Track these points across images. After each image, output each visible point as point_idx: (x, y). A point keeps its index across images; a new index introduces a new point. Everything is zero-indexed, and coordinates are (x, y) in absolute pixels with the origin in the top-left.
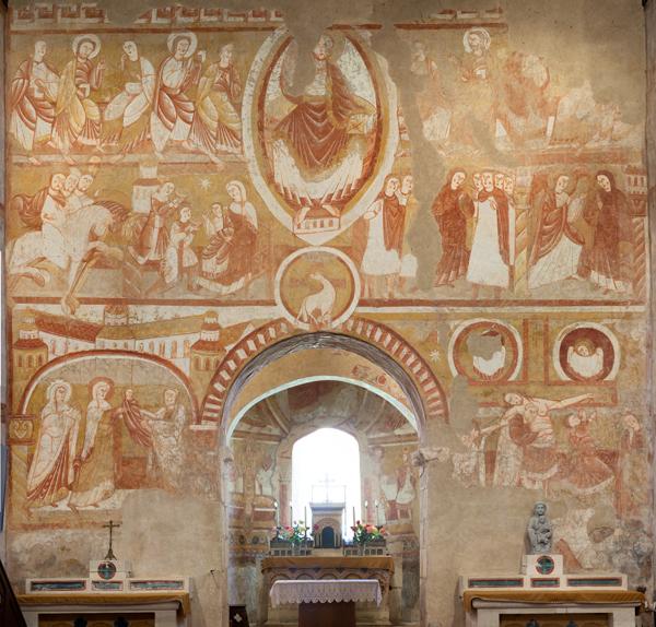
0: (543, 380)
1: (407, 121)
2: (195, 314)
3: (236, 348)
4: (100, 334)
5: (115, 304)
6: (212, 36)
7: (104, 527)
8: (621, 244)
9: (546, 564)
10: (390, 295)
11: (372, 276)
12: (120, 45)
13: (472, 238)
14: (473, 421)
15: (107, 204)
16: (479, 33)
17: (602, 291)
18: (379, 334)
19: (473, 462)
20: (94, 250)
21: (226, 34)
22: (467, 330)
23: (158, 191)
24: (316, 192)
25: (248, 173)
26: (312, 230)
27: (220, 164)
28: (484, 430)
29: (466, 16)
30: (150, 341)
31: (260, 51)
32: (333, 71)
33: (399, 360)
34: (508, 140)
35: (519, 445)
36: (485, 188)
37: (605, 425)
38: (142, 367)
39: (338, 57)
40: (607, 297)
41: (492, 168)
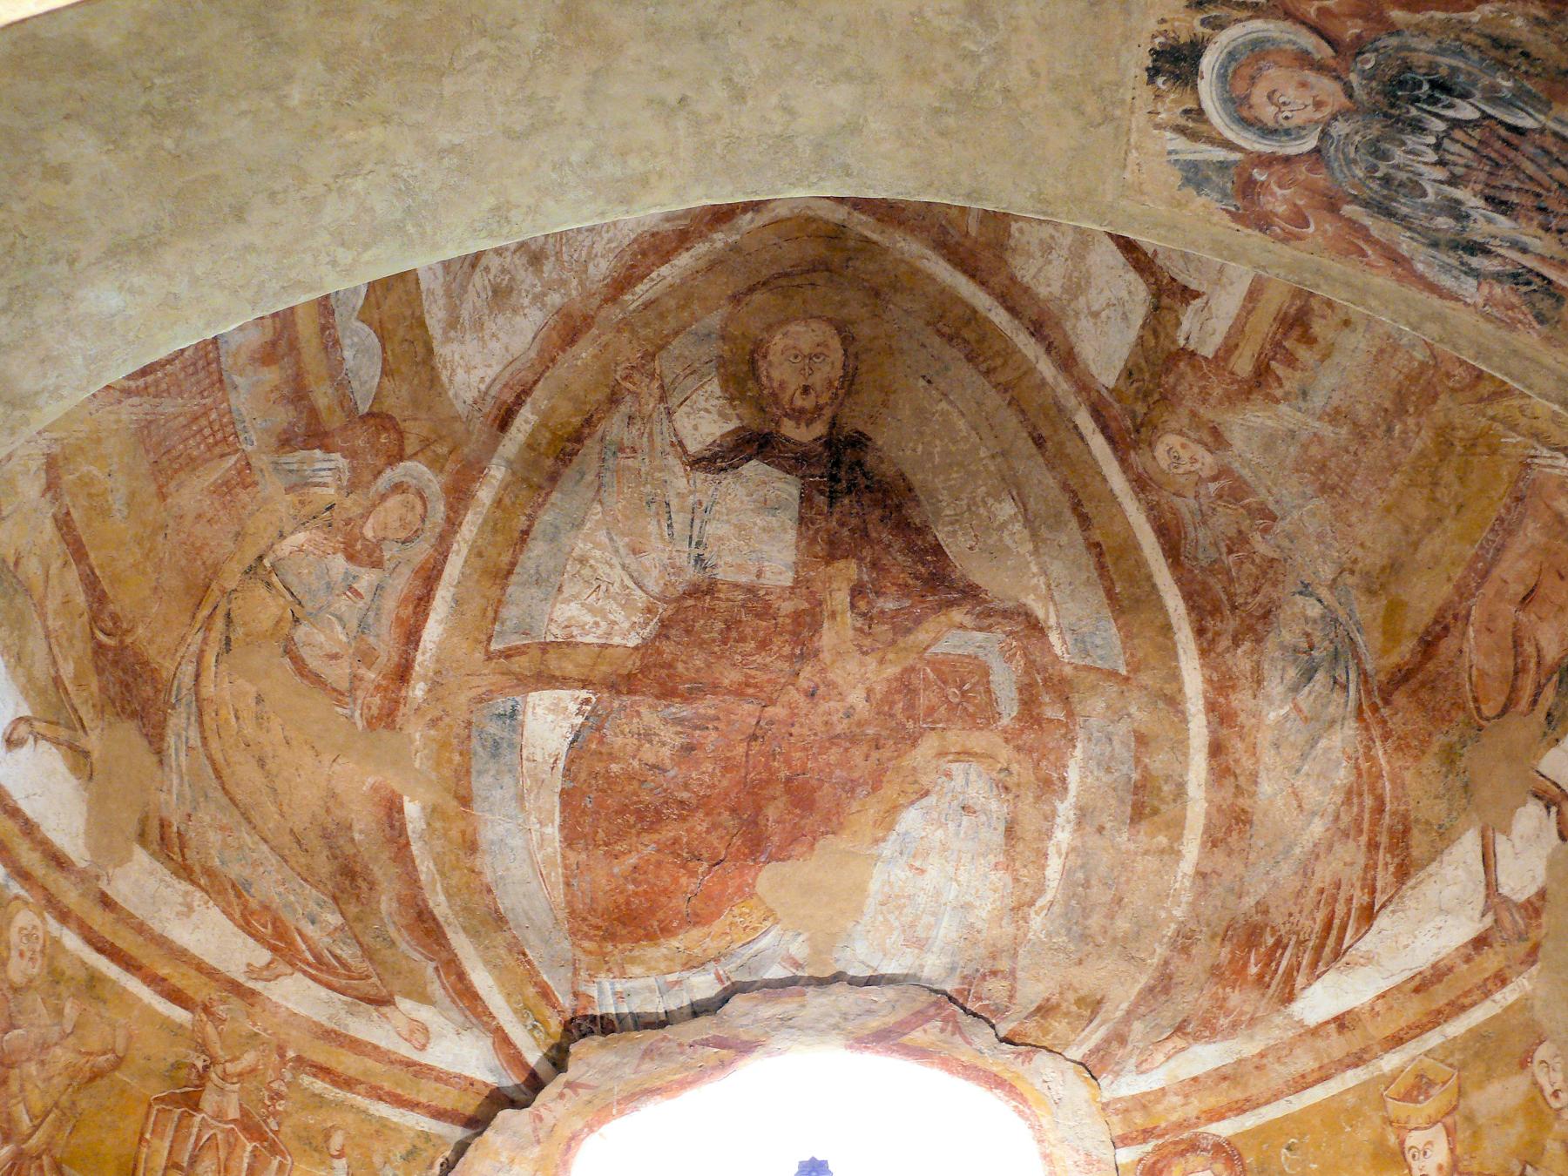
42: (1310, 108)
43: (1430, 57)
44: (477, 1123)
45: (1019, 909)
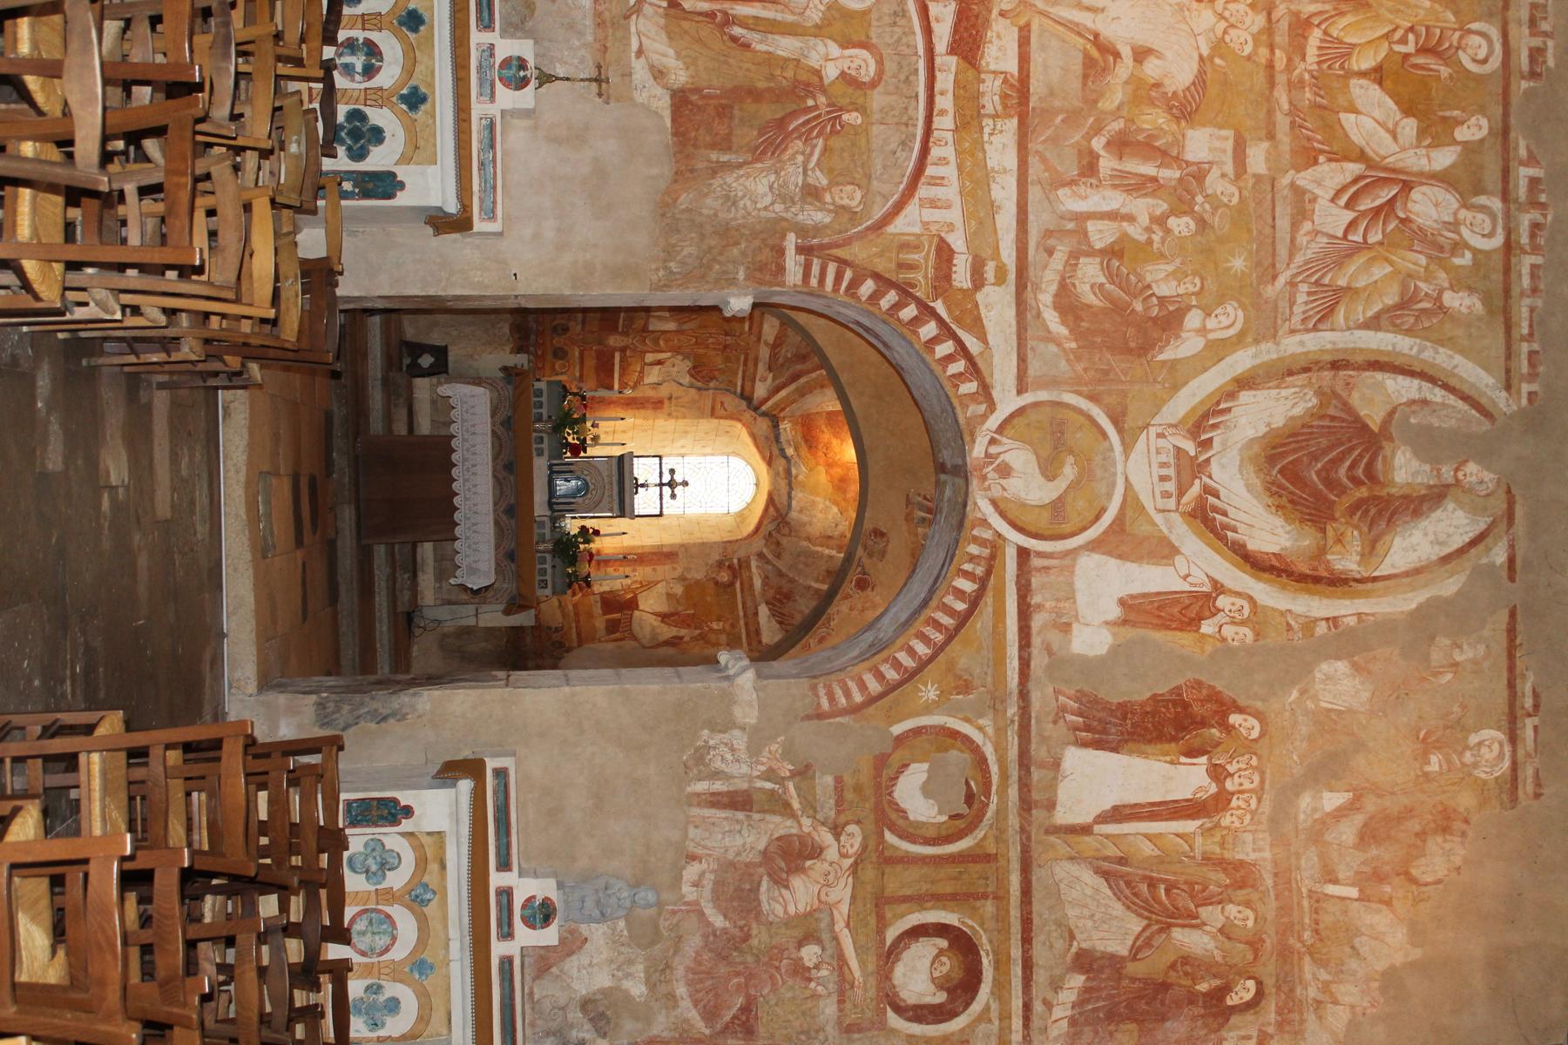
0: (888, 892)
1: (1351, 631)
2: (1002, 245)
3: (941, 321)
4: (964, 65)
5: (1019, 91)
6: (1497, 277)
7: (599, 67)
8: (1132, 1026)
9: (543, 914)
10: (1039, 607)
11: (1072, 573)
12: (1482, 110)
13: (1145, 755)
14: (808, 767)
15: (1200, 81)
16: (1501, 756)
17: (1050, 996)
18: (967, 586)
19: (733, 769)
20: (1117, 55)
21: (1499, 302)
22: (976, 750)
23: (1223, 175)
24: (1223, 467)
25: (1257, 341)
26: (1156, 460)
27: (1270, 291)
28: (791, 786)
29: (1529, 733)
30: (952, 158)
31: (1470, 365)
32: (1435, 496)
33: (919, 625)
34: (1317, 816)
35: (765, 853)
36: (1231, 775)
37: (804, 1013)
38: (903, 143)
39: (1461, 505)
40: (1038, 1007)
41: (1267, 786)
44: (742, 396)
45: (809, 539)
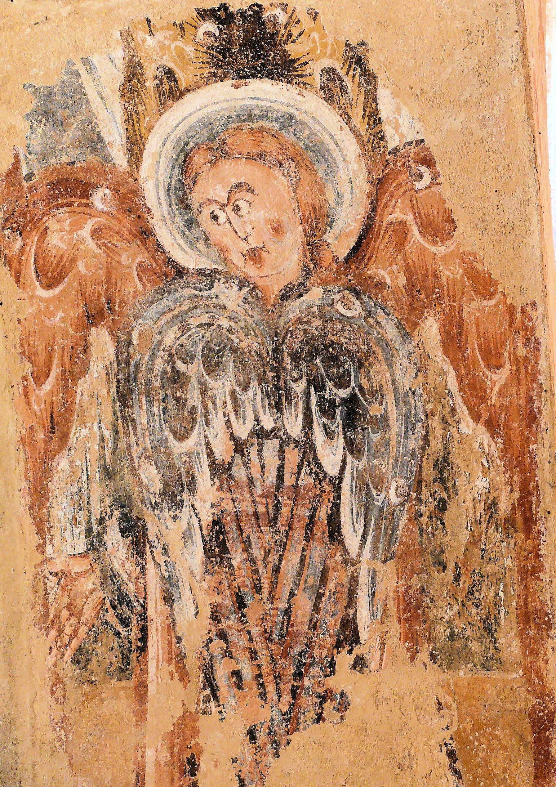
42: (245, 247)
43: (388, 388)
